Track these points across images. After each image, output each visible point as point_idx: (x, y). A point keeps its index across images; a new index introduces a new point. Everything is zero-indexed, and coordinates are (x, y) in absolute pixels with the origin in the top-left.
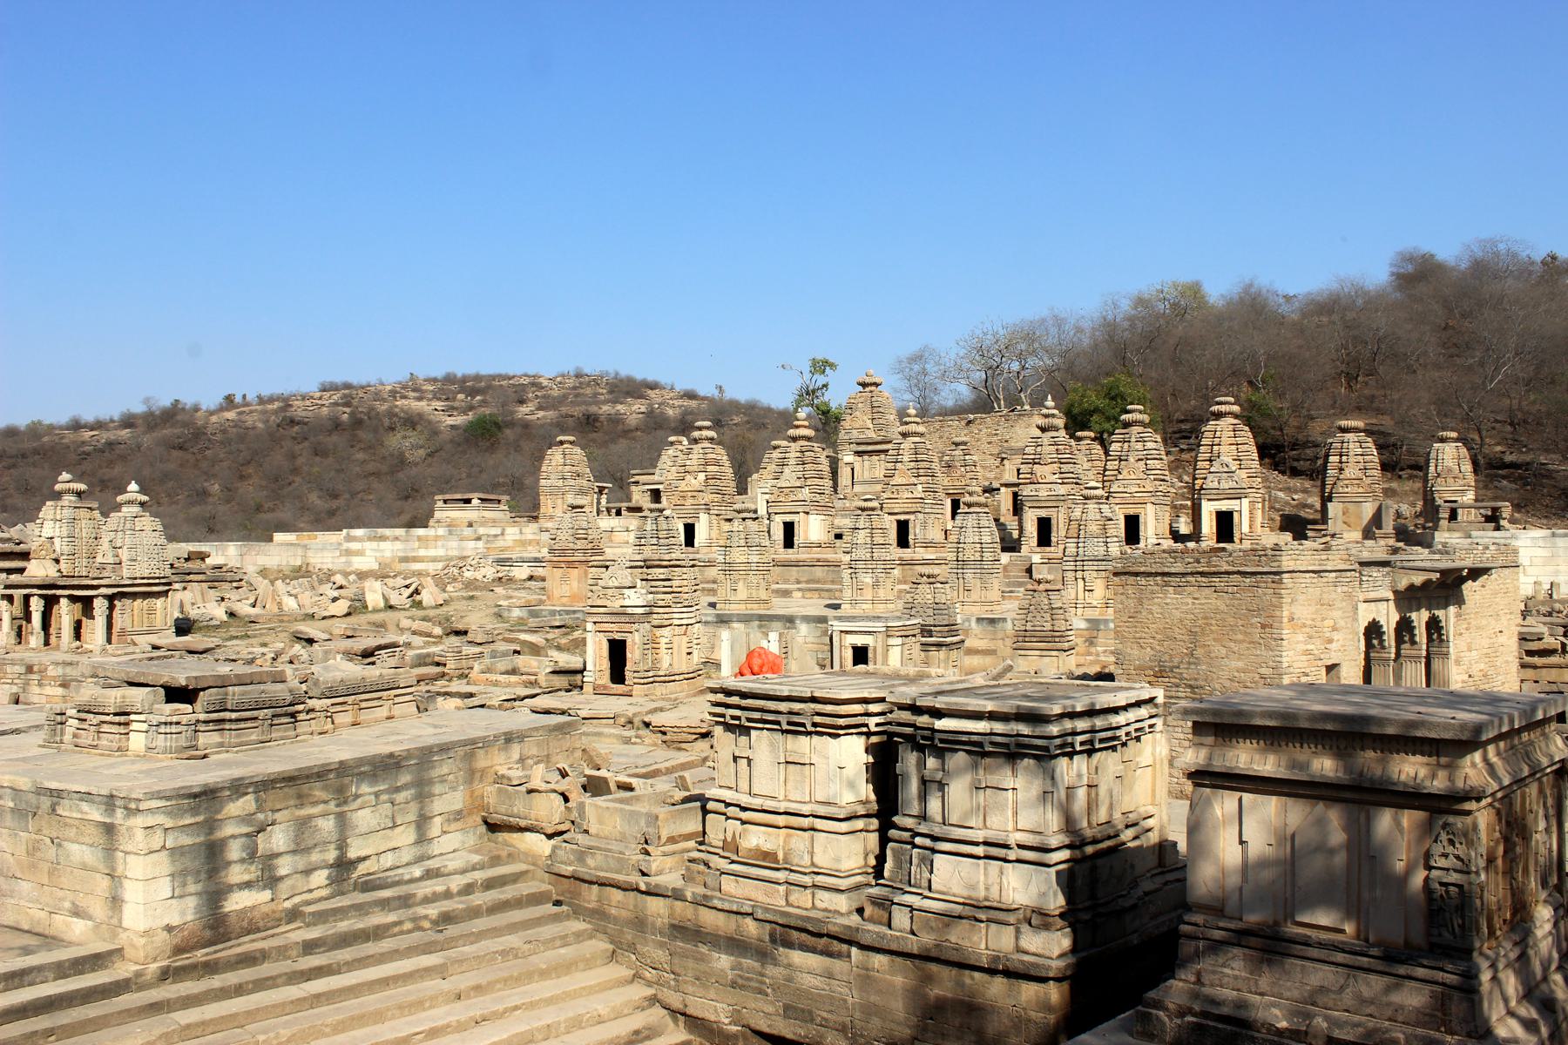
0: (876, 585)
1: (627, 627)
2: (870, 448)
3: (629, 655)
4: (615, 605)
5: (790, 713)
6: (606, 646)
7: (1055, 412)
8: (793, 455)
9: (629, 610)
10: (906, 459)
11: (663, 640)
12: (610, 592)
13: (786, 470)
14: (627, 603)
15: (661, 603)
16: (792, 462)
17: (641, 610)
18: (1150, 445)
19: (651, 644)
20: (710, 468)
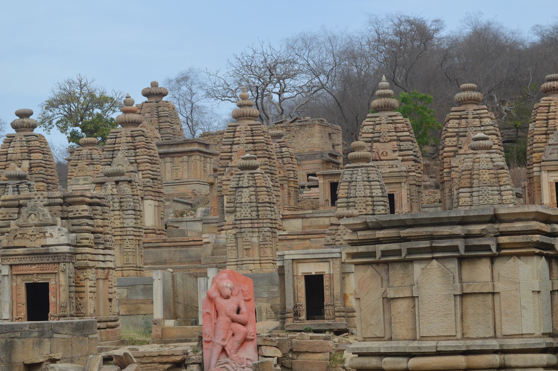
0: (262, 245)
1: (51, 268)
2: (172, 150)
3: (52, 299)
4: (38, 243)
5: (468, 236)
6: (23, 291)
7: (390, 91)
8: (123, 140)
9: (53, 249)
10: (243, 140)
11: (88, 283)
12: (30, 231)
13: (120, 155)
14: (49, 241)
15: (85, 242)
16: (123, 147)
17: (66, 249)
18: (487, 121)
19: (76, 287)
20: (33, 156)
